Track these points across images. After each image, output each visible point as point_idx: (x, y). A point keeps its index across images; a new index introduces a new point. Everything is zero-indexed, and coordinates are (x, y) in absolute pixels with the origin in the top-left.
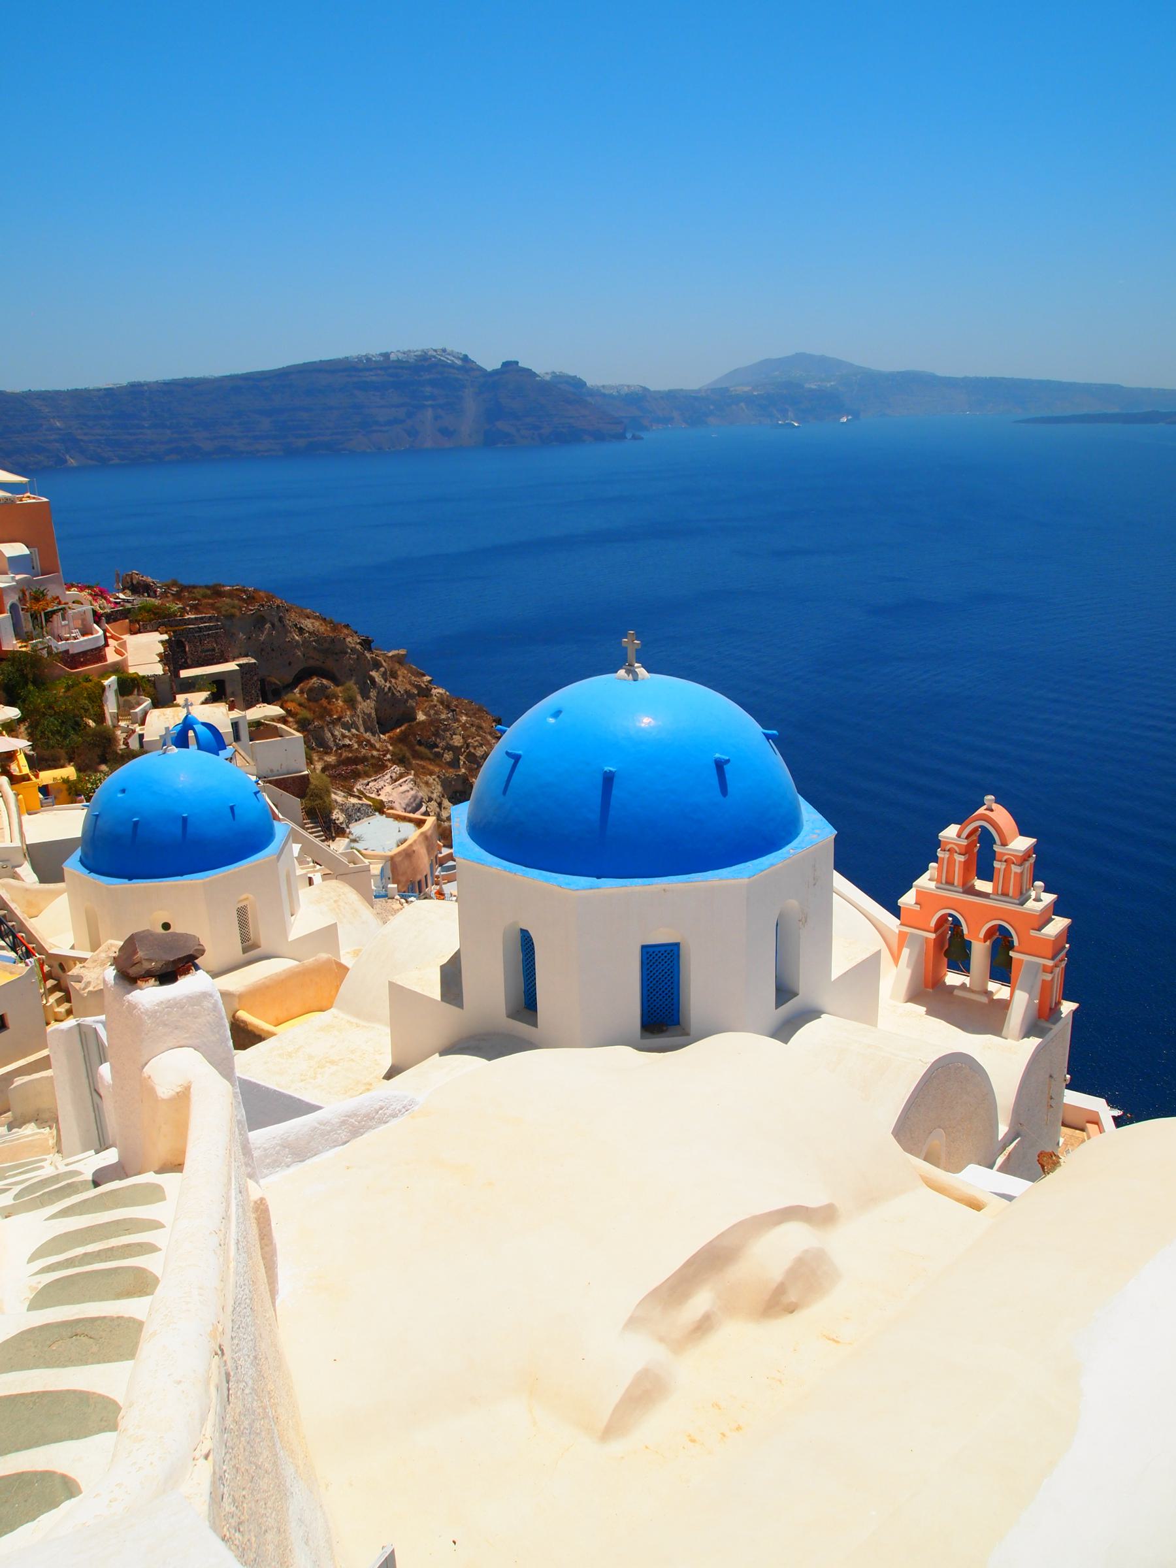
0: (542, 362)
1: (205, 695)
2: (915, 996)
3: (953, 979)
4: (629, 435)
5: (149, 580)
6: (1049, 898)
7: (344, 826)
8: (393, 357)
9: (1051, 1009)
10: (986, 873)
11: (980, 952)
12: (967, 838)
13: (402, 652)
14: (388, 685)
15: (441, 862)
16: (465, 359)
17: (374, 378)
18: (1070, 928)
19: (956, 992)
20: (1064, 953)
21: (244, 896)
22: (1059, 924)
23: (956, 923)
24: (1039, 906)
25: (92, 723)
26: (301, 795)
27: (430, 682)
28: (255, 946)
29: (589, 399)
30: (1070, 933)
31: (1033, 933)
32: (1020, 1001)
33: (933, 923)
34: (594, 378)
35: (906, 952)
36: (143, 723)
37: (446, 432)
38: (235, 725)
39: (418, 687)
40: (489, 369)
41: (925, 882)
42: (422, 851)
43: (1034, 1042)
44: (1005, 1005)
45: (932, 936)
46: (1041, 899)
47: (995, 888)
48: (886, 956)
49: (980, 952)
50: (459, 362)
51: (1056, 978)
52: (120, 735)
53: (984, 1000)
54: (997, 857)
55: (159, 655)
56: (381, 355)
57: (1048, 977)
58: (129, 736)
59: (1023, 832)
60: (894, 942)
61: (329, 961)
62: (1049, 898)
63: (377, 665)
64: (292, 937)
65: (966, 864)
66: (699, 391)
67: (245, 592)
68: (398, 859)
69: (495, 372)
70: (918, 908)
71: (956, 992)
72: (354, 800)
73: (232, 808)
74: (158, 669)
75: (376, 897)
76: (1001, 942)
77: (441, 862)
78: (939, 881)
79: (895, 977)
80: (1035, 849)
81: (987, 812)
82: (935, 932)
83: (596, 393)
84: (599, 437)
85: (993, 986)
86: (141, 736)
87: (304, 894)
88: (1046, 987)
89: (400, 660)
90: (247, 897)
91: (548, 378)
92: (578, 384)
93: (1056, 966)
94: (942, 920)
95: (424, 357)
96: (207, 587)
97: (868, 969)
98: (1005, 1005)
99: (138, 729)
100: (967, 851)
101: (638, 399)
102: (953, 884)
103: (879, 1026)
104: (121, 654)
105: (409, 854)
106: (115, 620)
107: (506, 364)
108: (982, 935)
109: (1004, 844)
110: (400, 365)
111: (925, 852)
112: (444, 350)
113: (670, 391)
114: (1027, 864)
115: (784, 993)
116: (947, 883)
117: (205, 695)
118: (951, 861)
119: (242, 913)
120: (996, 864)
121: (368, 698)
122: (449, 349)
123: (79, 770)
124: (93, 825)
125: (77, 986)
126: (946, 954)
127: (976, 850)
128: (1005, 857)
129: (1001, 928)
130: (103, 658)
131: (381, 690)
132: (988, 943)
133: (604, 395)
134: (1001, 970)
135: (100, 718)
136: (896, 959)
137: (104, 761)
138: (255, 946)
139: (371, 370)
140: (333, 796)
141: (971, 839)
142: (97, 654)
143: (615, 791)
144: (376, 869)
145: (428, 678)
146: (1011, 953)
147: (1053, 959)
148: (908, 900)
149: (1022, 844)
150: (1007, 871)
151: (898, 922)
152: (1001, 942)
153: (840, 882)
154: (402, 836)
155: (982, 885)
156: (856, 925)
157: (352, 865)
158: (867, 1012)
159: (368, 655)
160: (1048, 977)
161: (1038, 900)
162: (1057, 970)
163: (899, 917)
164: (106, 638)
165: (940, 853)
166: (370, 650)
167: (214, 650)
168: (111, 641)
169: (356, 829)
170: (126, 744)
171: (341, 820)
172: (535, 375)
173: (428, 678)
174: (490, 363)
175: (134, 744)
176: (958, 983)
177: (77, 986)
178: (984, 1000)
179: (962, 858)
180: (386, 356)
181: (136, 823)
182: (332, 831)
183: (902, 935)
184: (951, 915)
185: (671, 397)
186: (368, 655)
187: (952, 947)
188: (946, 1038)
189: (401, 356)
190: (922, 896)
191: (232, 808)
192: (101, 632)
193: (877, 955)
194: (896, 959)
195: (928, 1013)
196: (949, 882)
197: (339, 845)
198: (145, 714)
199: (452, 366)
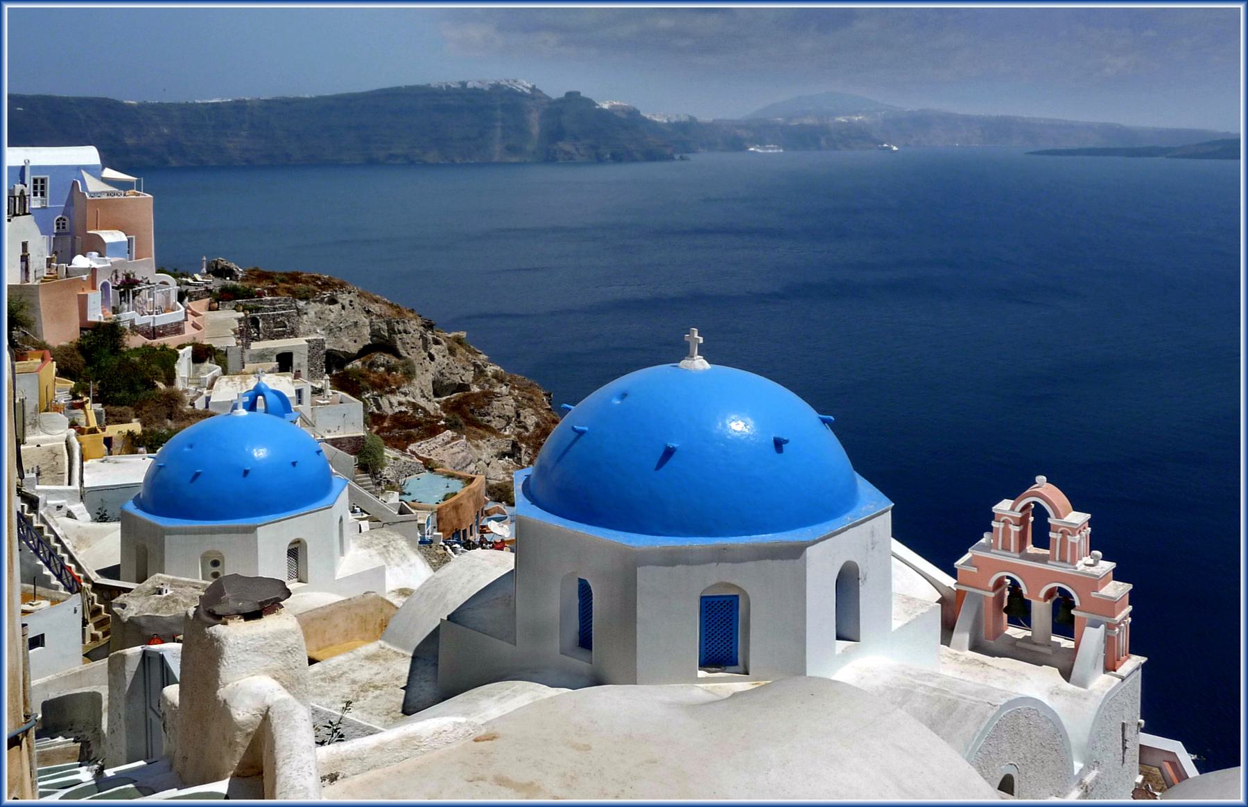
5: (233, 266)
19: (1018, 644)
23: (1015, 586)
25: (161, 386)
26: (353, 452)
31: (1093, 594)
36: (211, 386)
38: (299, 392)
45: (992, 595)
49: (1041, 611)
50: (528, 91)
52: (188, 397)
58: (196, 398)
59: (1077, 507)
67: (319, 279)
69: (560, 101)
74: (232, 342)
86: (208, 399)
94: (999, 583)
96: (286, 274)
100: (1023, 522)
106: (197, 299)
107: (569, 94)
108: (1042, 595)
111: (984, 523)
118: (1006, 531)
120: (1052, 535)
126: (1006, 610)
132: (1049, 602)
135: (170, 379)
137: (170, 417)
142: (177, 329)
146: (1073, 612)
149: (1079, 518)
150: (1064, 541)
154: (449, 491)
163: (956, 578)
164: (186, 314)
165: (994, 524)
168: (190, 316)
170: (193, 405)
179: (1018, 529)
192: (183, 309)
198: (215, 379)
199: (522, 94)
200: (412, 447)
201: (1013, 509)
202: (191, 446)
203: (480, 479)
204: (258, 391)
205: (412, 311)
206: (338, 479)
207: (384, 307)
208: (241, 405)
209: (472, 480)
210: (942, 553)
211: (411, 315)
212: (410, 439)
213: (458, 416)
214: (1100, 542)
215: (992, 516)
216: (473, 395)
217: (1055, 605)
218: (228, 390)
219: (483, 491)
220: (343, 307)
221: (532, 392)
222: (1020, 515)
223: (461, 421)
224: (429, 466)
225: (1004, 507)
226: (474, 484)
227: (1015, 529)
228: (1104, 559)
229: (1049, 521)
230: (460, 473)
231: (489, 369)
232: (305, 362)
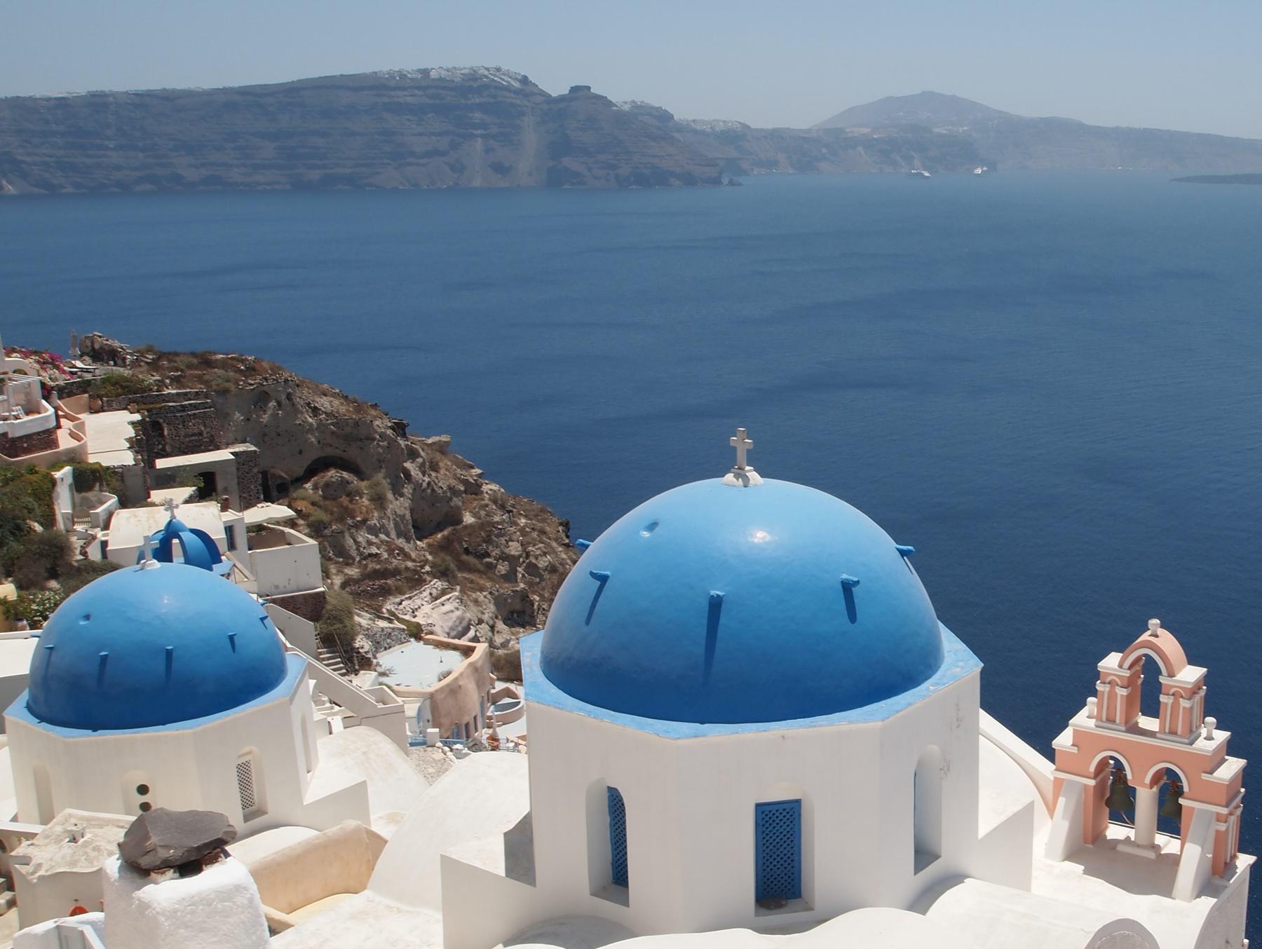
0: (620, 89)
1: (188, 491)
2: (1072, 855)
3: (1115, 832)
4: (725, 181)
5: (116, 344)
6: (1222, 736)
7: (370, 655)
8: (433, 74)
10: (1152, 709)
11: (1145, 800)
12: (1130, 668)
14: (427, 479)
15: (494, 699)
16: (525, 80)
17: (409, 99)
18: (1246, 772)
19: (1120, 848)
22: (1233, 766)
23: (1119, 767)
24: (1210, 746)
25: (38, 528)
26: (314, 617)
27: (480, 476)
28: (261, 812)
29: (676, 135)
30: (1246, 776)
31: (1205, 777)
32: (1190, 855)
33: (1092, 768)
34: (682, 111)
35: (1062, 801)
36: (106, 526)
37: (499, 169)
38: (229, 530)
39: (465, 482)
40: (554, 94)
41: (1083, 719)
42: (470, 686)
43: (1208, 902)
44: (1175, 860)
45: (1092, 783)
47: (1162, 725)
48: (1040, 806)
49: (1145, 800)
50: (517, 85)
51: (1231, 828)
52: (77, 543)
53: (1152, 855)
54: (1163, 690)
55: (129, 440)
56: (419, 71)
57: (1222, 827)
58: (88, 544)
59: (1193, 660)
61: (357, 830)
62: (1222, 736)
63: (413, 455)
64: (309, 797)
65: (1129, 700)
66: (810, 131)
67: (242, 361)
68: (439, 697)
69: (562, 99)
70: (1075, 750)
71: (1120, 848)
72: (383, 624)
74: (128, 458)
75: (411, 745)
76: (1169, 787)
77: (494, 699)
78: (1099, 718)
79: (1051, 831)
80: (1206, 679)
81: (1152, 639)
82: (1095, 778)
83: (683, 128)
84: (689, 180)
85: (1161, 839)
86: (104, 544)
87: (323, 745)
88: (1220, 838)
89: (442, 449)
91: (626, 108)
92: (665, 117)
93: (1231, 814)
94: (1103, 764)
95: (473, 76)
96: (194, 354)
97: (1020, 824)
98: (1175, 860)
99: (100, 534)
100: (1129, 683)
101: (735, 137)
102: (1114, 721)
104: (78, 439)
105: (454, 690)
106: (70, 395)
107: (574, 89)
108: (1148, 780)
109: (1171, 675)
110: (443, 85)
111: (1082, 686)
112: (498, 70)
113: (774, 130)
115: (924, 855)
116: (1108, 720)
117: (188, 491)
118: (1112, 695)
120: (1163, 698)
121: (402, 495)
122: (505, 68)
123: (20, 587)
124: (46, 657)
125: (23, 869)
126: (1107, 804)
127: (1140, 682)
129: (1169, 772)
130: (53, 443)
131: (417, 486)
132: (1155, 789)
133: (696, 132)
134: (1170, 819)
135: (49, 519)
136: (1051, 811)
137: (53, 575)
138: (261, 812)
139: (405, 89)
140: (357, 618)
141: (1134, 670)
142: (46, 438)
144: (411, 709)
146: (1181, 801)
147: (1227, 806)
148: (1063, 741)
149: (1191, 674)
150: (1175, 706)
151: (1054, 767)
152: (1169, 787)
153: (987, 722)
154: (445, 668)
157: (380, 706)
158: (1020, 877)
159: (402, 443)
160: (1222, 827)
161: (1209, 738)
162: (1233, 819)
164: (58, 417)
165: (1099, 686)
166: (404, 435)
167: (201, 434)
168: (63, 421)
169: (385, 659)
170: (84, 553)
171: (367, 648)
172: (610, 104)
174: (556, 86)
175: (94, 554)
176: (1122, 837)
177: (23, 869)
178: (1152, 855)
179: (1124, 692)
180: (425, 72)
182: (355, 662)
183: (1058, 783)
184: (1112, 758)
185: (775, 136)
186: (402, 443)
187: (1115, 797)
188: (1110, 902)
189: (443, 74)
191: (231, 638)
192: (51, 411)
193: (1030, 807)
194: (1051, 811)
195: (1085, 872)
197: (364, 681)
198: (110, 515)
199: (508, 89)
200: (389, 606)
201: (1120, 666)
202: (87, 617)
203: (481, 648)
204: (172, 531)
205: (375, 406)
206: (296, 660)
207: (336, 402)
208: (149, 554)
209: (472, 649)
210: (1038, 729)
211: (373, 412)
212: (386, 592)
213: (448, 558)
214: (1218, 701)
215: (1097, 675)
216: (466, 527)
217: (1162, 792)
218: (131, 528)
219: (488, 667)
220: (279, 404)
221: (544, 521)
222: (1127, 674)
223: (452, 566)
224: (416, 633)
225: (1111, 662)
226: (476, 656)
227: (1122, 692)
228: (1219, 727)
229: (1162, 680)
230: (456, 641)
231: (485, 488)
232: (233, 484)
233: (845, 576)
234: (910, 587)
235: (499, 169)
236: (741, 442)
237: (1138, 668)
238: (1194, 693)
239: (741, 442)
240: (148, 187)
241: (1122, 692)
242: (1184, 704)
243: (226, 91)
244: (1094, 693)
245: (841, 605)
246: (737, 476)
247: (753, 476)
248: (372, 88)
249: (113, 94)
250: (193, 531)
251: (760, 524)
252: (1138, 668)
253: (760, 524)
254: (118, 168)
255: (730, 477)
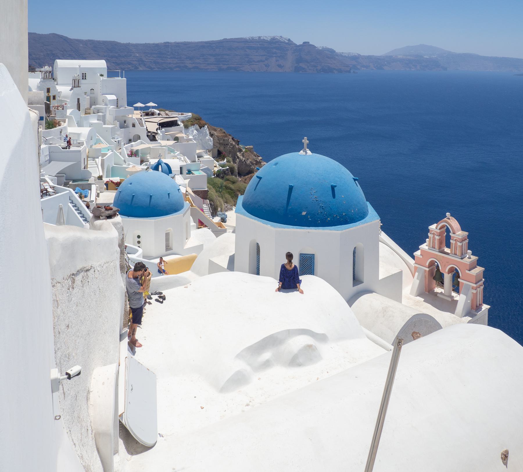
2: (420, 294)
4: (352, 71)
8: (262, 38)
9: (477, 306)
10: (448, 245)
11: (448, 278)
12: (440, 229)
13: (251, 147)
14: (244, 159)
16: (289, 40)
17: (254, 45)
20: (482, 282)
21: (169, 229)
22: (479, 270)
27: (261, 159)
29: (336, 57)
31: (467, 272)
33: (427, 264)
34: (339, 49)
35: (417, 274)
37: (280, 66)
39: (256, 161)
40: (298, 44)
41: (424, 247)
45: (427, 269)
46: (470, 258)
47: (451, 251)
49: (448, 278)
50: (287, 42)
53: (450, 299)
57: (475, 292)
60: (413, 270)
62: (474, 258)
63: (240, 151)
66: (381, 56)
69: (300, 45)
70: (421, 257)
73: (169, 194)
76: (456, 275)
79: (410, 285)
82: (428, 268)
83: (341, 55)
85: (454, 294)
89: (250, 150)
90: (170, 229)
91: (320, 48)
100: (440, 234)
102: (435, 248)
103: (403, 303)
107: (304, 43)
108: (447, 271)
110: (264, 41)
112: (281, 37)
113: (369, 56)
114: (464, 242)
115: (356, 280)
116: (433, 247)
119: (167, 235)
120: (451, 241)
121: (236, 163)
128: (455, 239)
131: (240, 161)
133: (342, 56)
134: (456, 288)
143: (293, 193)
145: (260, 158)
146: (459, 280)
147: (476, 284)
148: (417, 253)
150: (456, 244)
152: (456, 275)
155: (447, 250)
156: (390, 257)
159: (237, 146)
160: (475, 292)
161: (469, 258)
163: (414, 259)
165: (429, 235)
166: (238, 145)
173: (260, 158)
174: (298, 42)
178: (450, 299)
180: (260, 37)
181: (133, 196)
183: (416, 268)
186: (237, 146)
190: (423, 252)
196: (434, 247)
199: (284, 42)
201: (436, 228)
215: (428, 231)
222: (439, 231)
225: (433, 227)
227: (437, 238)
229: (451, 234)
233: (332, 184)
234: (358, 191)
235: (280, 66)
236: (305, 141)
237: (443, 230)
238: (463, 241)
239: (305, 141)
240: (178, 69)
241: (437, 238)
242: (459, 244)
243: (201, 42)
244: (428, 237)
245: (330, 193)
246: (304, 151)
247: (309, 152)
248: (243, 42)
249: (171, 43)
250: (165, 163)
251: (307, 166)
252: (443, 230)
253: (307, 166)
254: (170, 63)
255: (302, 151)
